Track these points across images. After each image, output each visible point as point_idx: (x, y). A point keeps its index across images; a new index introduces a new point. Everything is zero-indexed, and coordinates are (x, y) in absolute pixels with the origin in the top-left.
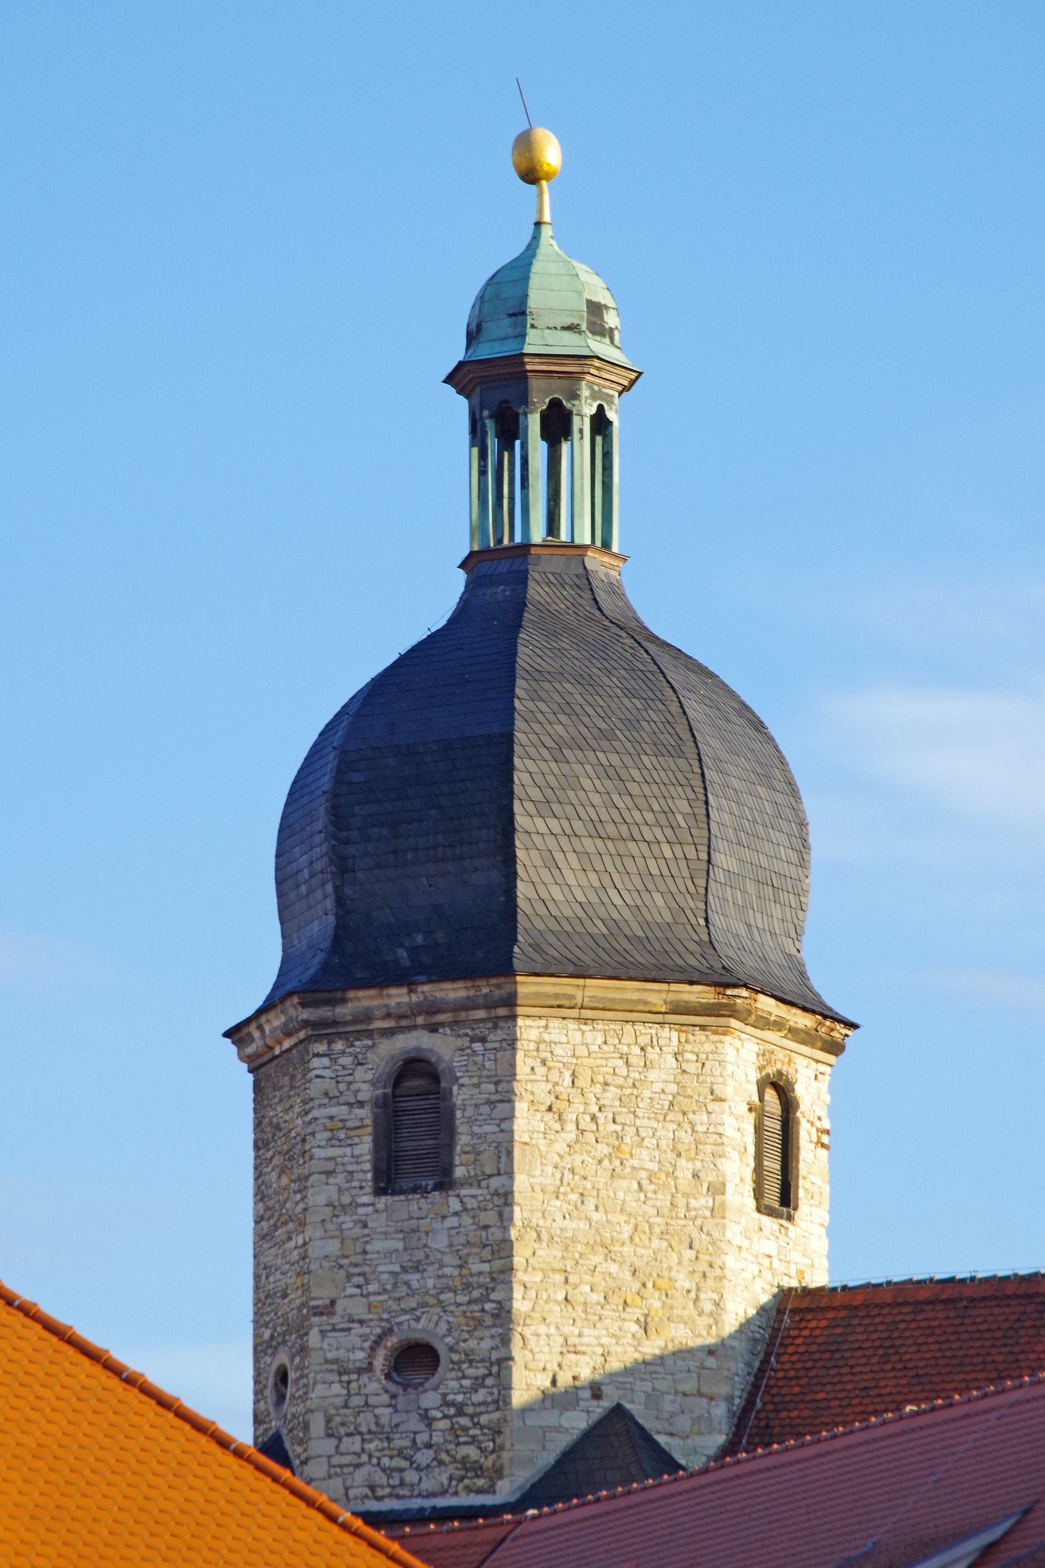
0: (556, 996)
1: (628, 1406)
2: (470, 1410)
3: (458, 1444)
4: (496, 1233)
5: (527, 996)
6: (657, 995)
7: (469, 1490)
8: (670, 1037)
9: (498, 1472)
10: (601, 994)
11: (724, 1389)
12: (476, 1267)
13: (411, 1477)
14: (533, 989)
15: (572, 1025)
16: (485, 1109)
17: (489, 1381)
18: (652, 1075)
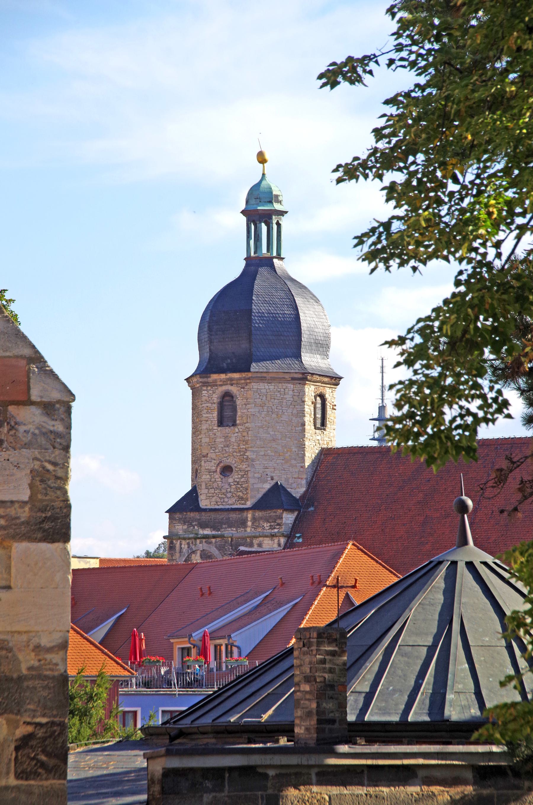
2: (240, 483)
7: (240, 504)
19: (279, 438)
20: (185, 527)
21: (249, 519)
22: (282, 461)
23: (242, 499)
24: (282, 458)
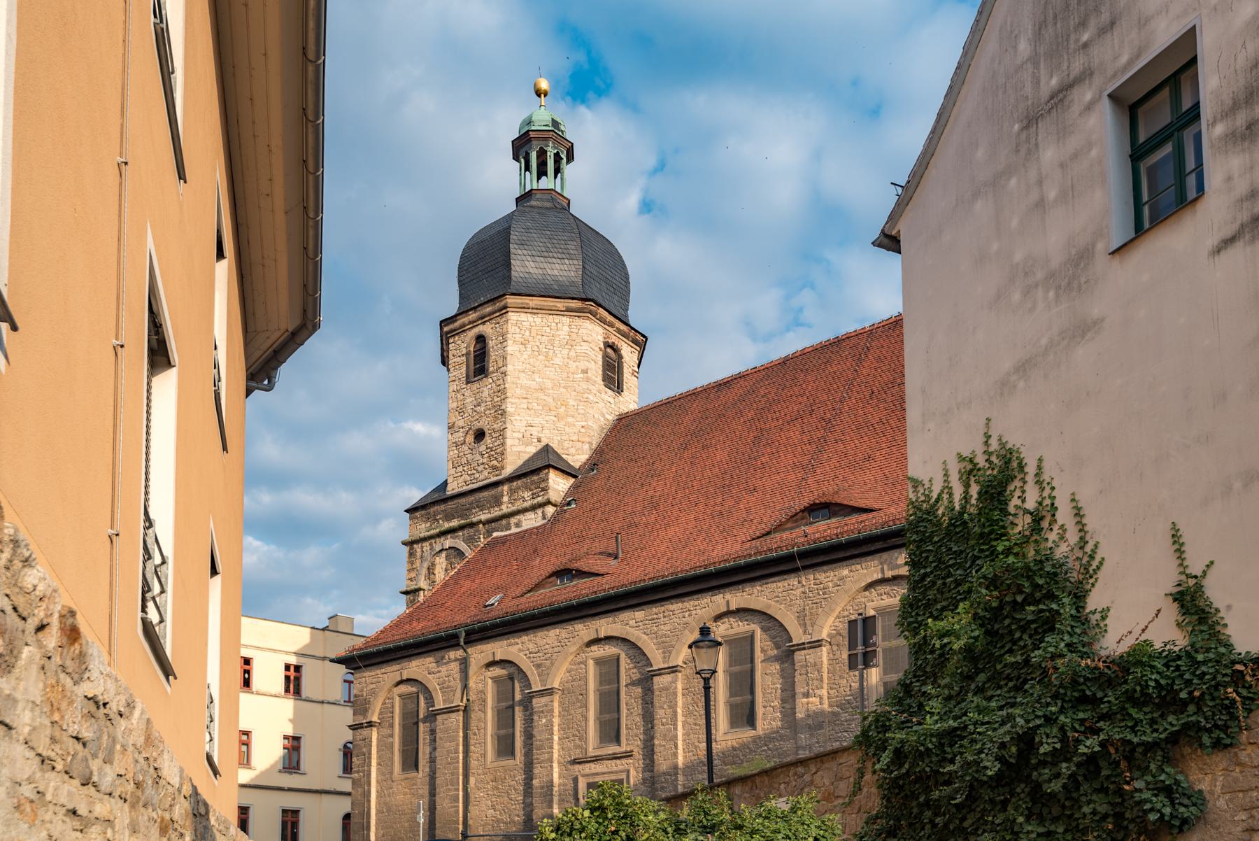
0: (522, 303)
1: (551, 445)
4: (502, 387)
5: (511, 303)
6: (561, 304)
7: (493, 476)
8: (566, 320)
9: (503, 468)
10: (539, 303)
11: (588, 440)
12: (496, 399)
13: (477, 475)
14: (513, 301)
15: (529, 315)
16: (499, 346)
17: (500, 437)
18: (559, 333)
19: (550, 387)
21: (505, 493)
22: (554, 418)
23: (494, 468)
24: (554, 413)
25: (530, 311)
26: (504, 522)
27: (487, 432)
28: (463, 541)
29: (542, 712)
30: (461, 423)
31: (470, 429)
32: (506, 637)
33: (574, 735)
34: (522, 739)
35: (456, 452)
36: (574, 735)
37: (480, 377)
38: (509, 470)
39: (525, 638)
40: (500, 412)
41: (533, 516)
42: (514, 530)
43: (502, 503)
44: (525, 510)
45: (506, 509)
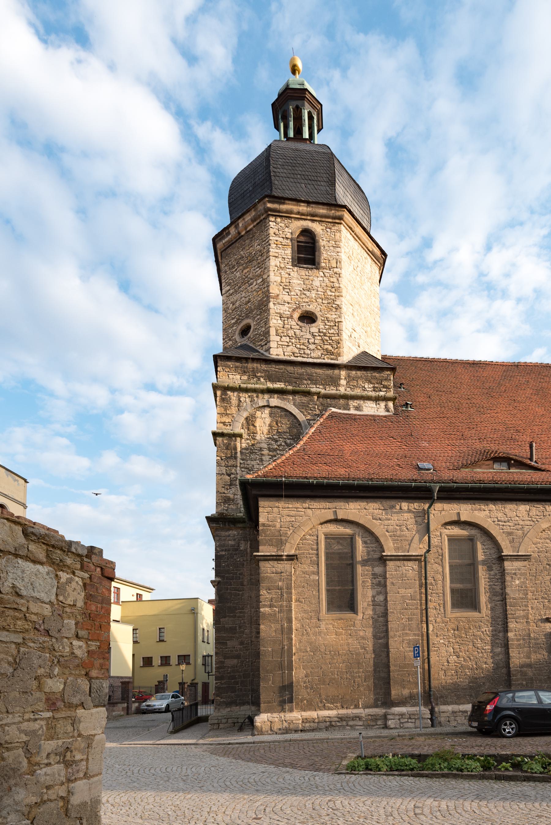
3: (324, 344)
7: (328, 358)
13: (308, 352)
20: (245, 378)
25: (353, 234)
26: (342, 401)
27: (320, 318)
28: (294, 404)
29: (515, 574)
30: (287, 298)
31: (299, 308)
32: (472, 501)
33: (543, 598)
34: (488, 595)
35: (280, 321)
36: (543, 598)
37: (310, 266)
38: (346, 357)
39: (492, 506)
40: (334, 306)
41: (375, 406)
42: (352, 411)
43: (339, 385)
44: (369, 398)
45: (342, 390)
